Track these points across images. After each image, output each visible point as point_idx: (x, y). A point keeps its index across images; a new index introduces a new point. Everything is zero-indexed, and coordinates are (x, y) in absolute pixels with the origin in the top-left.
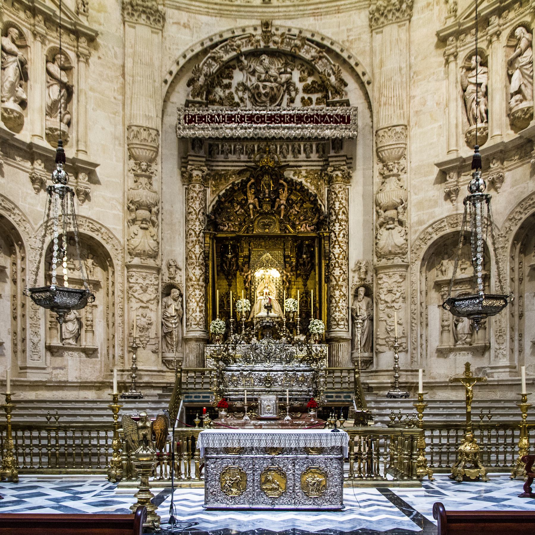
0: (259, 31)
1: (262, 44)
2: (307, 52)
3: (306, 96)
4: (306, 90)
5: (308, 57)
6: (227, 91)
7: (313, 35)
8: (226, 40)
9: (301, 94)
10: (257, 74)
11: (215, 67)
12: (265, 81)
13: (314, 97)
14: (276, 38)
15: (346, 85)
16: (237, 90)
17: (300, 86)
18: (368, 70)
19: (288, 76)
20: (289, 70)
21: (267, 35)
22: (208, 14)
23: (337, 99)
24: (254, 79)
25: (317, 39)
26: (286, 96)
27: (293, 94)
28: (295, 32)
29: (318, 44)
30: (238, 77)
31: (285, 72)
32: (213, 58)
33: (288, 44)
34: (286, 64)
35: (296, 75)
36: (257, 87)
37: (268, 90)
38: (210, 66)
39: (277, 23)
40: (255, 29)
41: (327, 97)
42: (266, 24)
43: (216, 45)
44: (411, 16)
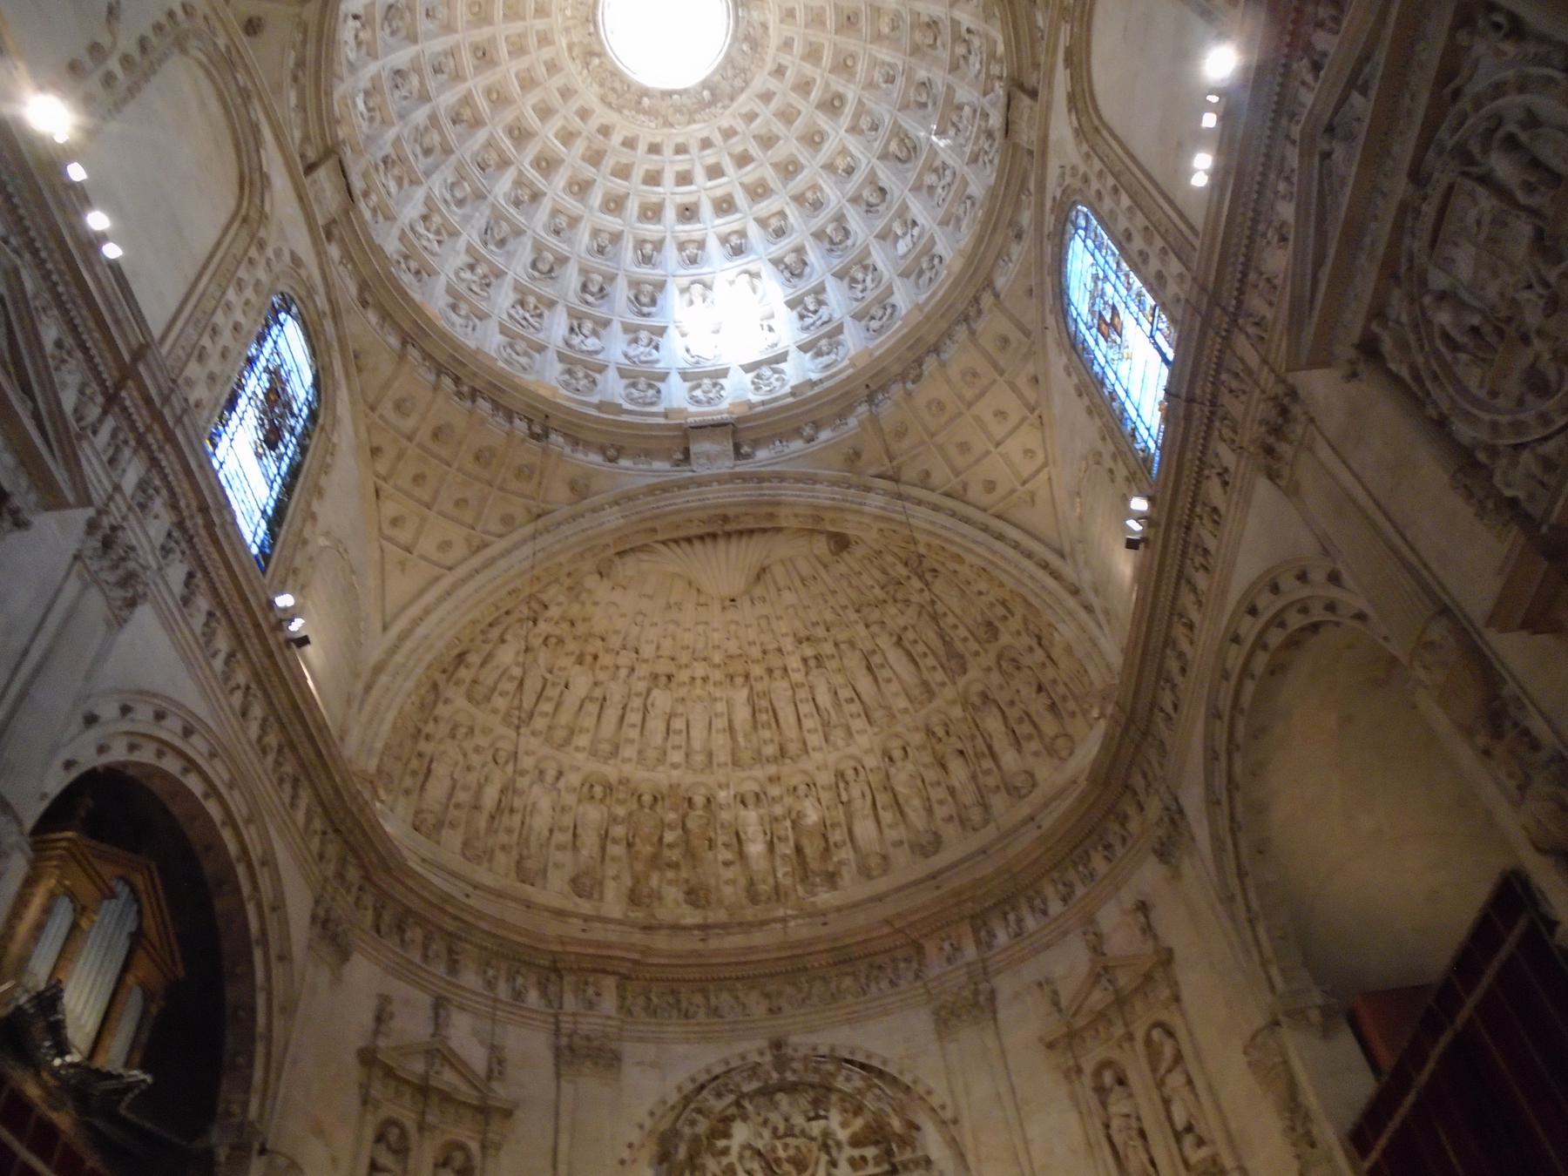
0: (768, 1058)
1: (775, 1075)
2: (848, 1079)
3: (856, 1153)
4: (856, 1142)
5: (847, 1088)
6: (725, 1161)
7: (852, 1053)
8: (717, 1077)
9: (849, 1152)
10: (770, 1125)
11: (703, 1126)
12: (786, 1135)
13: (870, 1152)
14: (796, 1065)
15: (918, 1128)
16: (741, 1157)
17: (843, 1135)
18: (949, 1102)
19: (822, 1122)
20: (822, 1113)
21: (781, 1063)
22: (688, 1041)
23: (907, 1155)
24: (766, 1133)
25: (860, 1058)
26: (824, 1158)
27: (834, 1152)
28: (824, 1050)
29: (863, 1066)
30: (741, 1133)
31: (817, 1117)
32: (699, 1111)
33: (816, 1071)
34: (816, 1103)
35: (835, 1119)
36: (774, 1149)
37: (792, 1152)
38: (693, 1123)
39: (794, 1039)
40: (761, 1053)
41: (889, 1153)
42: (777, 1045)
43: (702, 1087)
44: (994, 1012)
